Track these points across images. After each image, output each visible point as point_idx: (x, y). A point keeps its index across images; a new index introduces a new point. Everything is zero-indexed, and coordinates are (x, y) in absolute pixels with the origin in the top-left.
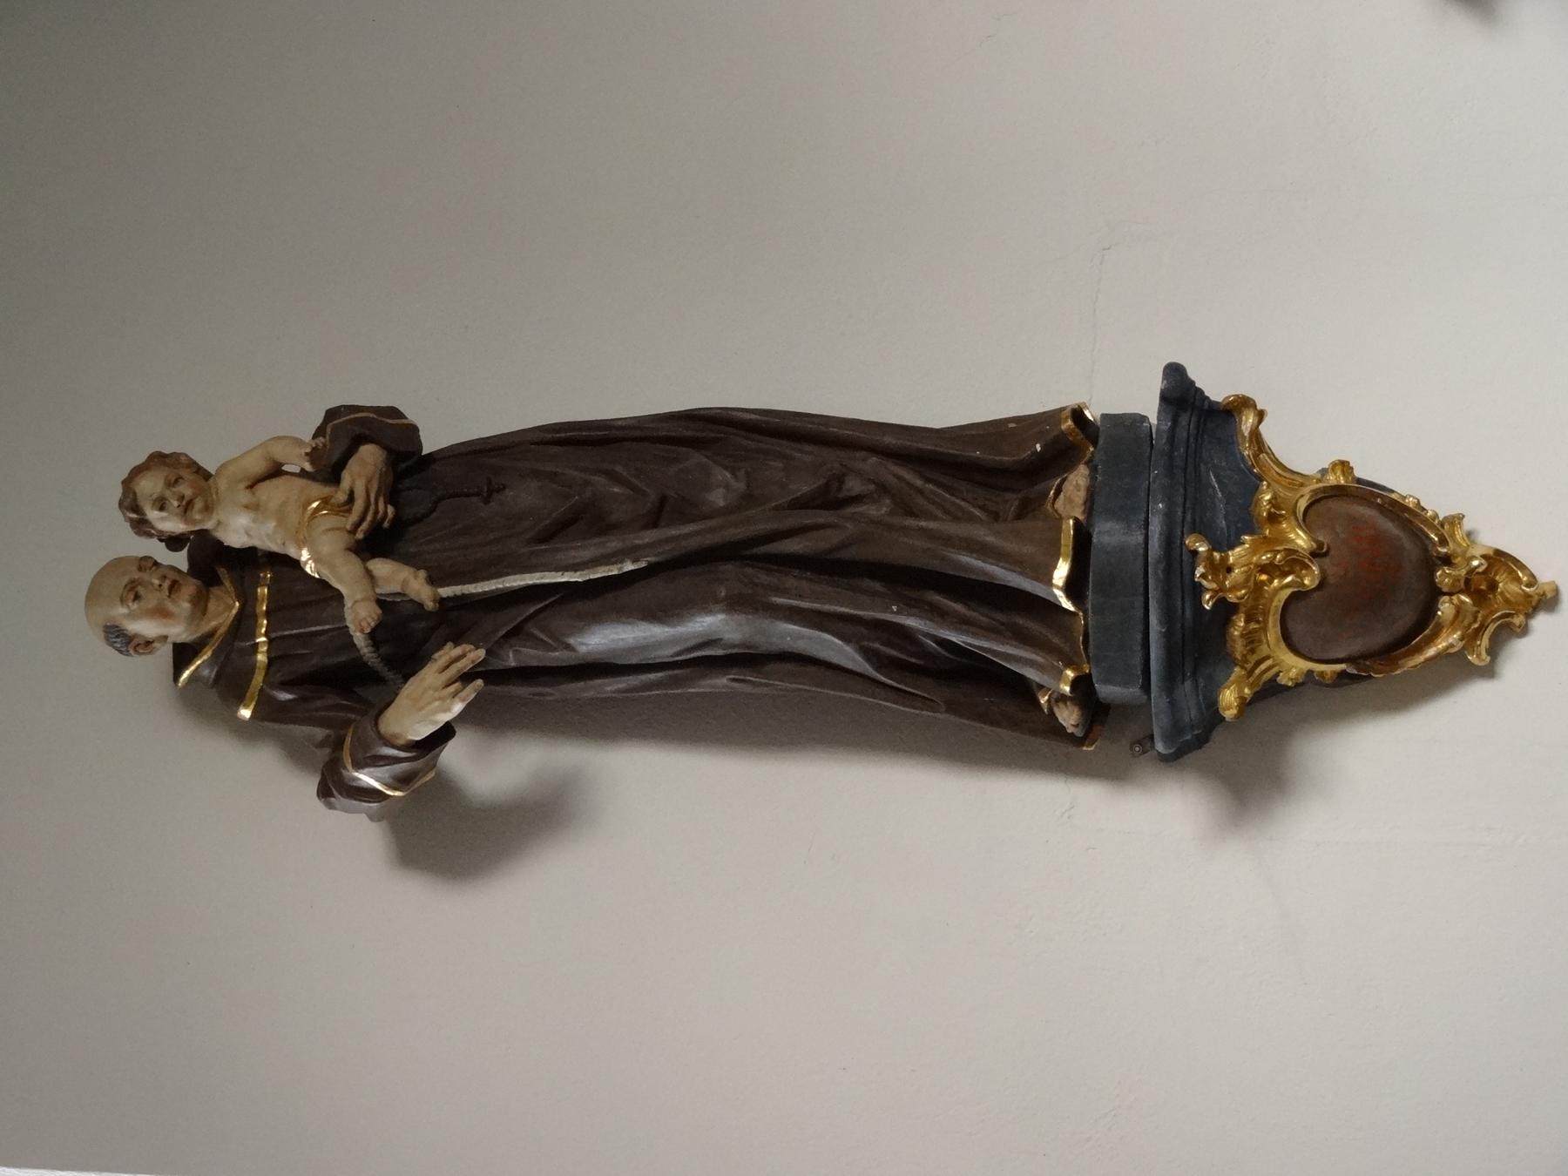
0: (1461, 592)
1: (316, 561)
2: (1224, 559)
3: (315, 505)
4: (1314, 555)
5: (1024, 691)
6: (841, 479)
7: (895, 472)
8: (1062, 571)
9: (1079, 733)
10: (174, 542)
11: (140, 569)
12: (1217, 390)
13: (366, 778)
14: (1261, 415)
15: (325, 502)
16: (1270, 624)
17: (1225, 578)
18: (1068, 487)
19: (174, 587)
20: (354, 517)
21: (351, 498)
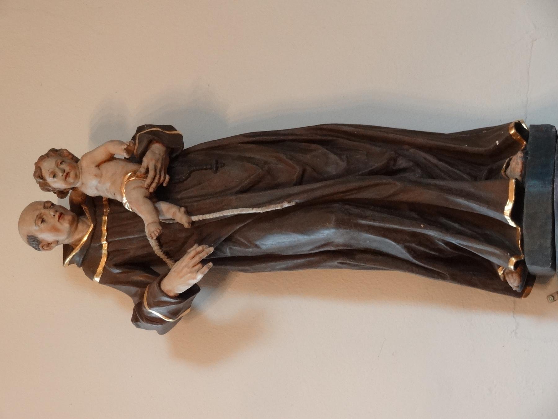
1: (129, 202)
3: (129, 174)
6: (395, 160)
7: (422, 155)
8: (509, 207)
9: (518, 290)
10: (62, 194)
11: (45, 207)
13: (155, 313)
15: (135, 173)
18: (513, 164)
19: (61, 216)
20: (148, 181)
21: (147, 171)
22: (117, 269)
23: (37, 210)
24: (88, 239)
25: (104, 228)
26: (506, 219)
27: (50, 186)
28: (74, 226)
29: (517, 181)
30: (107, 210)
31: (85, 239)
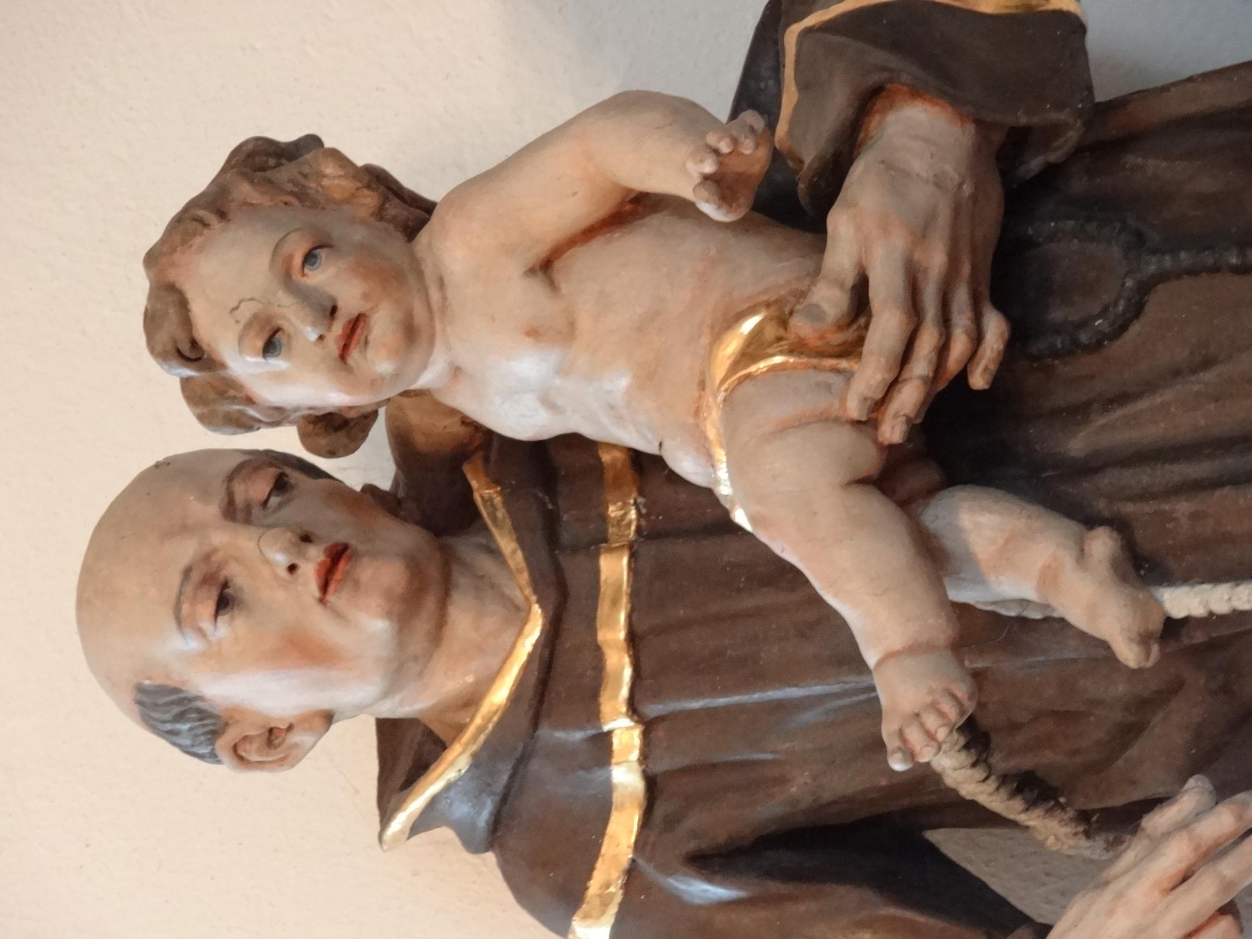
3: (749, 325)
20: (869, 374)
22: (710, 880)
23: (184, 529)
24: (516, 697)
25: (613, 632)
27: (250, 401)
28: (422, 625)
30: (624, 513)
31: (500, 694)
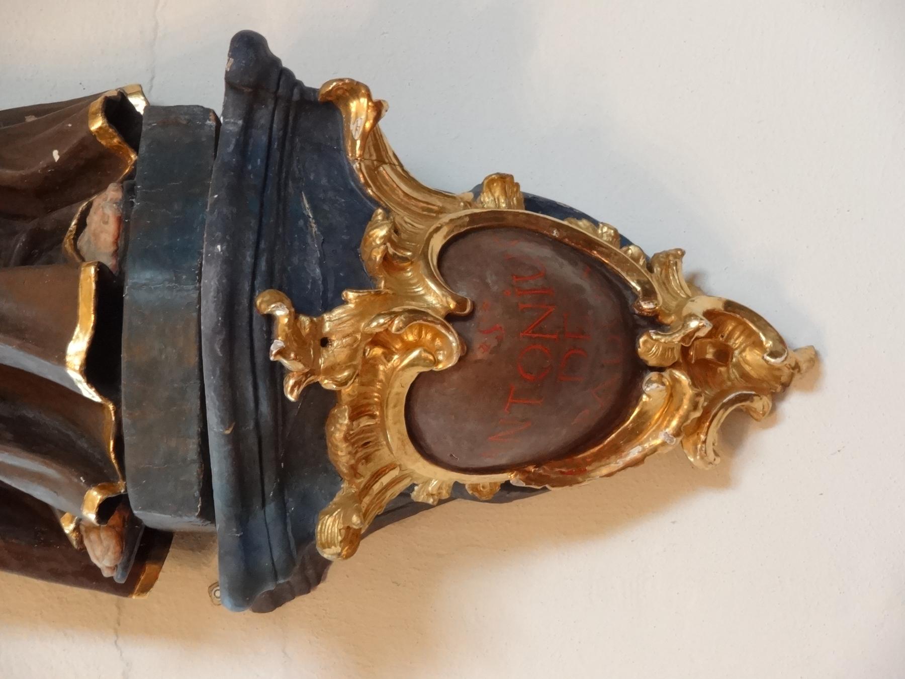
0: (675, 366)
2: (317, 327)
4: (451, 318)
5: (43, 520)
8: (78, 347)
9: (119, 578)
12: (313, 75)
14: (378, 108)
16: (390, 422)
17: (318, 355)
18: (94, 220)
26: (71, 380)
29: (102, 271)
